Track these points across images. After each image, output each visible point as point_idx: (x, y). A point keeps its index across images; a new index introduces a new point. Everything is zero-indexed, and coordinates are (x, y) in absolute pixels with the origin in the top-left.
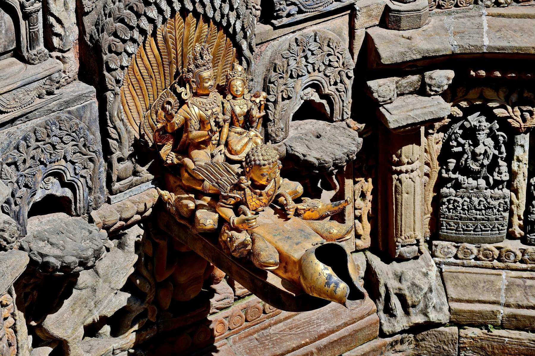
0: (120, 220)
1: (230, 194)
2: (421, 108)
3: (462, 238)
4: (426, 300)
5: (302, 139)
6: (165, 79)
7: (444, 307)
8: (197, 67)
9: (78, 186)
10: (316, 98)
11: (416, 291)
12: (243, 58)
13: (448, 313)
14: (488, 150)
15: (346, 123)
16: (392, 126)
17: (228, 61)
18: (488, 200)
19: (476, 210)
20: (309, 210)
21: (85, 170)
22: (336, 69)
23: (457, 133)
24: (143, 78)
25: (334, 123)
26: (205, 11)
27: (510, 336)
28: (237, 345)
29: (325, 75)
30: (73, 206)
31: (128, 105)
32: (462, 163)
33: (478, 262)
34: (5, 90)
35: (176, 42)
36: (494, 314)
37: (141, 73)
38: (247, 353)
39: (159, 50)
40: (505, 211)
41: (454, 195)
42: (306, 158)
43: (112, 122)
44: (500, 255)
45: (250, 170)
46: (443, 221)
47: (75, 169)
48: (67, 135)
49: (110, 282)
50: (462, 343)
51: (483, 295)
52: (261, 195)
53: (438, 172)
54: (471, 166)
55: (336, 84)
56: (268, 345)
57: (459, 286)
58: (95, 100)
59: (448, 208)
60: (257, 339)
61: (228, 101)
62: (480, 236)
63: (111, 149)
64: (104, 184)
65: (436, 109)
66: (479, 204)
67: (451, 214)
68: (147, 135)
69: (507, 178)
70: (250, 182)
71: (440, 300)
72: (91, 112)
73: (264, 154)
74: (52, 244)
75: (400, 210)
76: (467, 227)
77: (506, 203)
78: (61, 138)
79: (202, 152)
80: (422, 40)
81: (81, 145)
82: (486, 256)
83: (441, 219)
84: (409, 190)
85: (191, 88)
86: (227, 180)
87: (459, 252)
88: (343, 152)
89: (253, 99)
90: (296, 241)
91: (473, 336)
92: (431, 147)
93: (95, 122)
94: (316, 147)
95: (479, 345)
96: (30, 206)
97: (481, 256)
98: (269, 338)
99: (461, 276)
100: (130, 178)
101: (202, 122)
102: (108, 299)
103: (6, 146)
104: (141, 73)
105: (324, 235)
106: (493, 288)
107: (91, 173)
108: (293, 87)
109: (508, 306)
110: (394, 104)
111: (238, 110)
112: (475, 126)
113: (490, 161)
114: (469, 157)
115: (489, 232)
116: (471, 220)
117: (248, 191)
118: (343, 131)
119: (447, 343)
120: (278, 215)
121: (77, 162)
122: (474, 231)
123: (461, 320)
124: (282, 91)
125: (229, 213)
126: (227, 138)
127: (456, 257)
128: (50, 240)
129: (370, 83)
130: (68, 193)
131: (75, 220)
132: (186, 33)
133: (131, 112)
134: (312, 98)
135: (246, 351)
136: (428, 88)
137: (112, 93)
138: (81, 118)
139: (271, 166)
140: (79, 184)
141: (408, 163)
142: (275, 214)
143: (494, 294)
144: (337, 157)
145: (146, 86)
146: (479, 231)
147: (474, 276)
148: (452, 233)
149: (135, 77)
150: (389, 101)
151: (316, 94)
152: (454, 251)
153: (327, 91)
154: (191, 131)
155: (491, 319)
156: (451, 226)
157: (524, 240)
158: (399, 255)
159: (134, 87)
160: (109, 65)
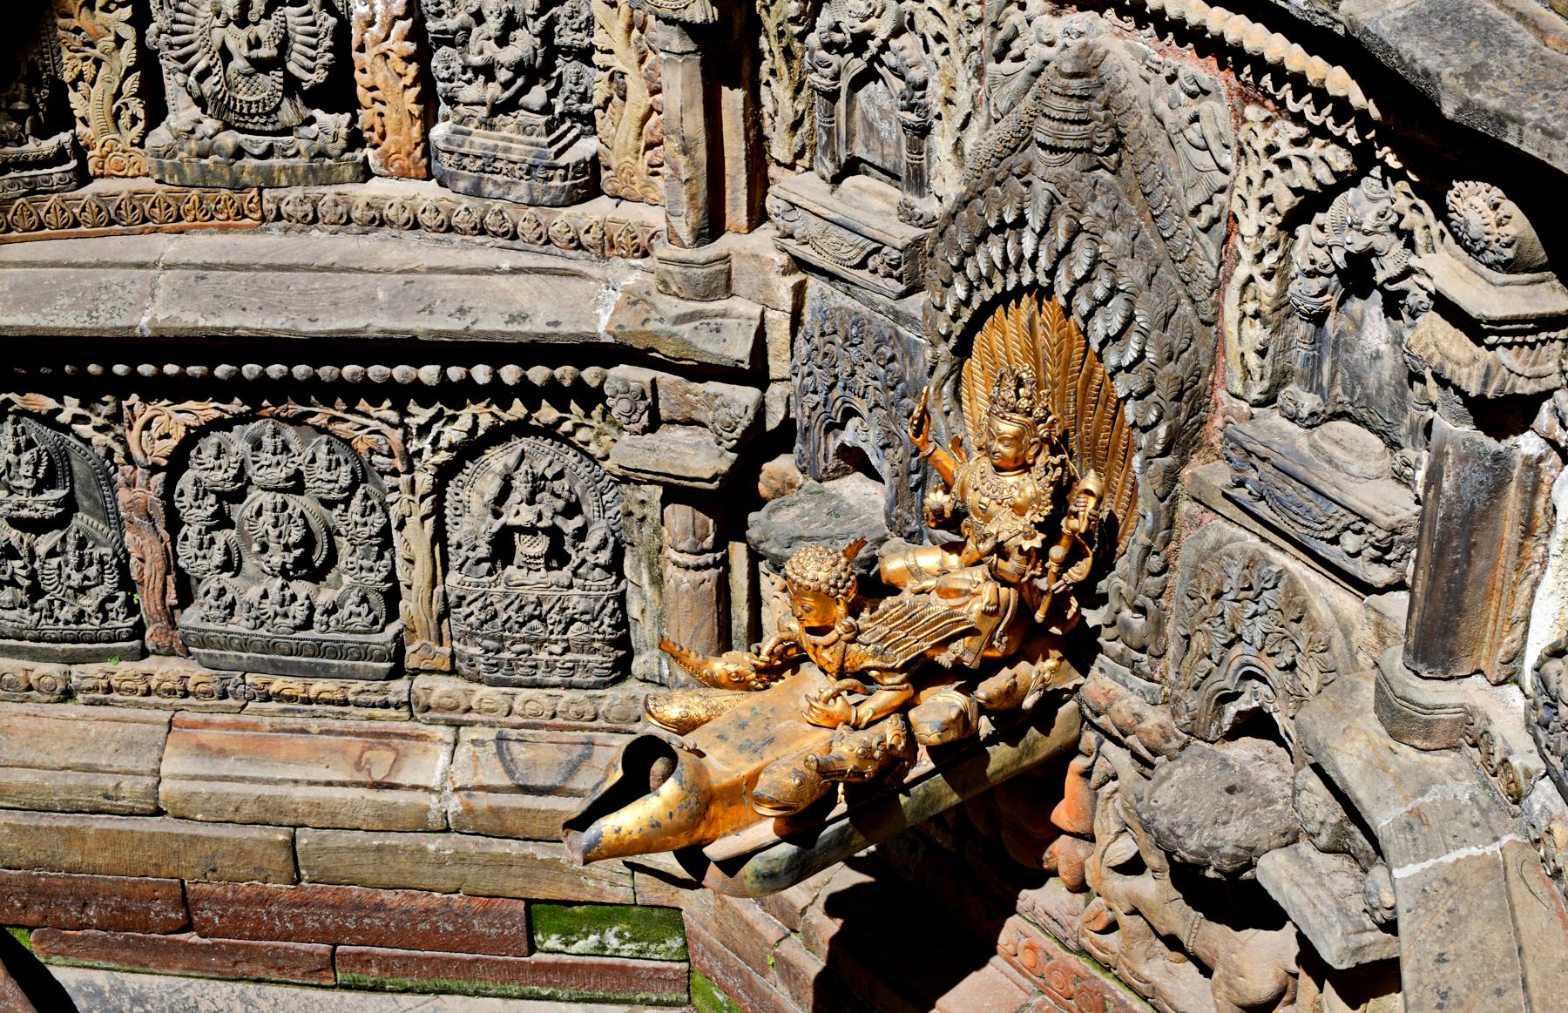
34: (815, 210)
80: (1359, 757)
96: (838, 443)
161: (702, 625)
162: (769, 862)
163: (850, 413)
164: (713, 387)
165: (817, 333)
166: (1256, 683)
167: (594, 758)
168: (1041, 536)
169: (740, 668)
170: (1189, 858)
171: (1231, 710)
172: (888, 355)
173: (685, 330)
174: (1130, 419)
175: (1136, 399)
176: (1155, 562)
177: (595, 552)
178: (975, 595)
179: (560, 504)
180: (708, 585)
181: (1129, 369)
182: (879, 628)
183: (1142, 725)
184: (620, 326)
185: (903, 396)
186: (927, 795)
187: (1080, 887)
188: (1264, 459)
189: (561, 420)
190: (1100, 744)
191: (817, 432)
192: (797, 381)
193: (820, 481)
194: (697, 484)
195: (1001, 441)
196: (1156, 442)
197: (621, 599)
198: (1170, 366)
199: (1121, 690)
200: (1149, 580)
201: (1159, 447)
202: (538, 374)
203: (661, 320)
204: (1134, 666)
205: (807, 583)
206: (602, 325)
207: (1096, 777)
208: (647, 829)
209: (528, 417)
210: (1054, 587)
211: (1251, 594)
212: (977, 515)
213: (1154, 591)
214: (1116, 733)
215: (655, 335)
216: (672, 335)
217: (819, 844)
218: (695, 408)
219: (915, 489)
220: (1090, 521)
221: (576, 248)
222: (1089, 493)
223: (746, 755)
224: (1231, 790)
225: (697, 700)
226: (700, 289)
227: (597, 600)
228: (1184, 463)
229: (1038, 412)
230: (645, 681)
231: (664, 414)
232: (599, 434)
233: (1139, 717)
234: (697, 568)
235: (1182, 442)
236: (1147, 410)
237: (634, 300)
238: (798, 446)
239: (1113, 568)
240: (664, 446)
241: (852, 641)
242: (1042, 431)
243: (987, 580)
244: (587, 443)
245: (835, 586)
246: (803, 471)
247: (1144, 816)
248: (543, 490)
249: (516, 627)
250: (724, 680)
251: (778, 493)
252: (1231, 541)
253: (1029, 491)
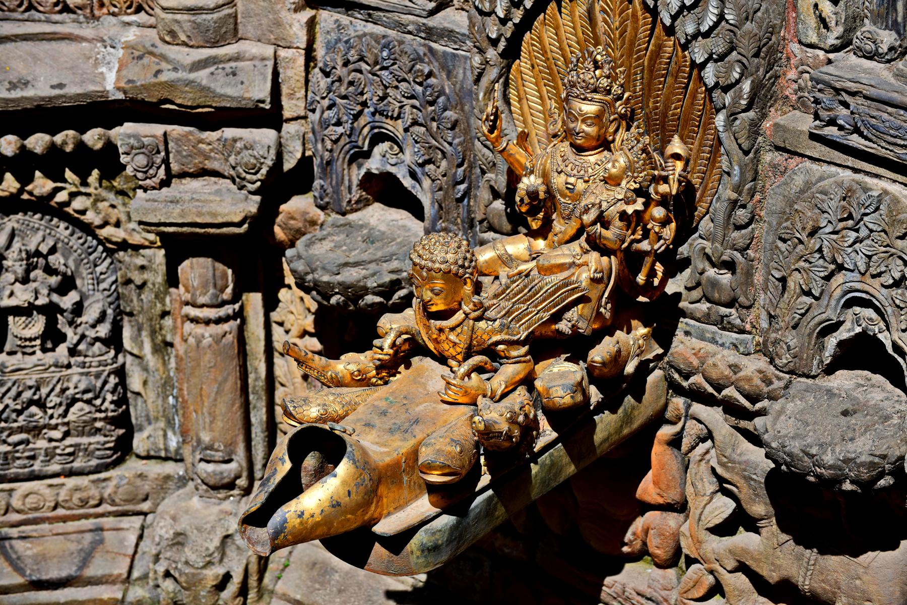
26: (656, 6)
48: (404, 80)
96: (363, 172)
103: (333, 41)
107: (440, 177)
134: (880, 336)
161: (225, 380)
162: (433, 534)
163: (378, 138)
164: (229, 133)
165: (340, 62)
166: (857, 309)
167: (107, 540)
168: (641, 200)
169: (361, 367)
170: (826, 473)
171: (831, 342)
172: (426, 71)
173: (202, 76)
174: (710, 80)
175: (716, 61)
176: (741, 215)
177: (94, 326)
178: (579, 266)
179: (54, 280)
180: (230, 337)
181: (706, 35)
182: (503, 304)
183: (741, 374)
184: (129, 81)
185: (445, 110)
186: (553, 464)
187: (675, 559)
188: (853, 94)
189: (57, 190)
190: (689, 407)
191: (340, 165)
192: (315, 117)
193: (344, 214)
194: (225, 230)
195: (583, 121)
196: (741, 97)
197: (121, 373)
198: (748, 25)
199: (711, 347)
200: (736, 234)
201: (744, 102)
202: (38, 142)
203: (175, 69)
204: (723, 323)
205: (437, 265)
206: (110, 82)
207: (686, 443)
208: (328, 510)
209: (21, 191)
210: (656, 247)
211: (850, 223)
212: (564, 196)
213: (741, 243)
214: (710, 390)
215: (170, 85)
216: (189, 83)
217: (472, 515)
218: (207, 157)
219: (460, 200)
220: (680, 182)
221: (60, 12)
222: (677, 157)
223: (398, 436)
224: (845, 413)
225: (331, 398)
226: (210, 34)
227: (98, 376)
228: (764, 116)
229: (616, 89)
230: (148, 457)
231: (175, 167)
232: (96, 201)
233: (735, 368)
234: (219, 321)
235: (762, 98)
236: (730, 69)
237: (137, 53)
238: (317, 183)
239: (696, 230)
240: (187, 197)
241: (479, 319)
242: (621, 109)
243: (586, 252)
244: (83, 212)
245: (463, 266)
246: (322, 208)
247: (774, 445)
248: (35, 267)
249: (14, 416)
250: (348, 378)
251: (300, 233)
252: (821, 179)
253: (622, 161)
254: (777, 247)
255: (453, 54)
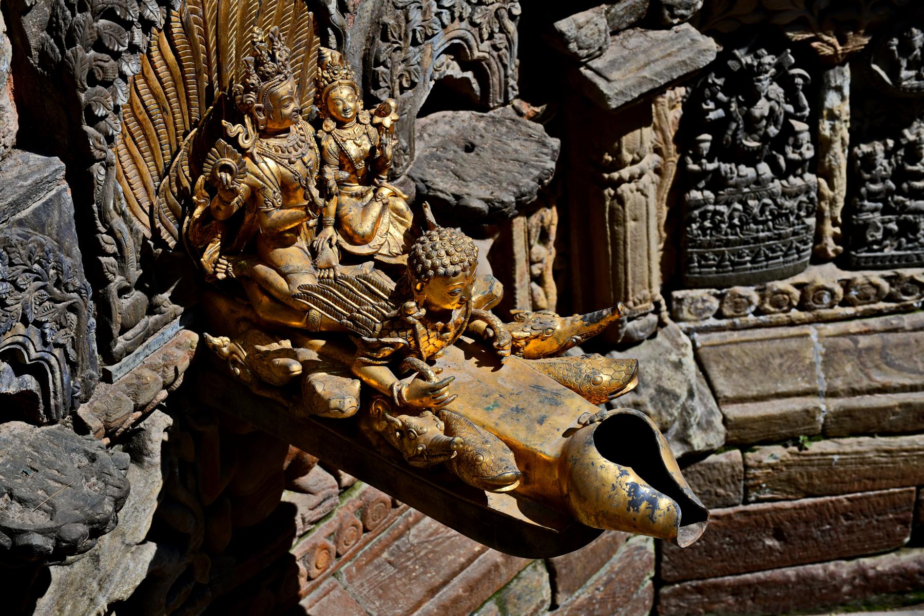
0: (136, 409)
1: (383, 340)
2: (663, 58)
3: (730, 278)
4: (685, 414)
5: (439, 159)
6: (189, 106)
7: (713, 419)
8: (264, 77)
9: (51, 367)
10: (455, 70)
11: (667, 403)
12: (329, 29)
13: (722, 428)
14: (777, 108)
15: (513, 107)
16: (613, 104)
17: (300, 40)
18: (779, 200)
19: (757, 222)
20: (536, 337)
21: (62, 332)
22: (490, 7)
23: (714, 84)
24: (150, 116)
25: (491, 113)
27: (841, 450)
28: (357, 583)
29: (473, 24)
30: (41, 406)
31: (127, 178)
32: (727, 140)
33: (762, 318)
35: (206, 29)
36: (809, 414)
37: (145, 106)
38: (380, 597)
39: (175, 51)
40: (808, 216)
41: (712, 201)
42: (463, 203)
43: (105, 222)
44: (803, 298)
45: (422, 287)
46: (692, 253)
47: (43, 336)
48: (25, 271)
49: (123, 535)
50: (752, 479)
51: (783, 382)
52: (445, 330)
53: (676, 161)
54: (744, 142)
55: (491, 37)
56: (414, 570)
57: (732, 372)
58: (65, 185)
59: (702, 228)
60: (390, 562)
61: (329, 133)
62: (765, 269)
63: (106, 276)
64: (95, 346)
65: (691, 55)
66: (762, 211)
67: (708, 238)
68: (166, 228)
69: (809, 154)
70: (423, 312)
71: (705, 405)
72: (60, 212)
73: (452, 250)
74: (21, 501)
75: (622, 253)
76: (740, 256)
77: (811, 200)
78: (14, 283)
79: (292, 249)
81: (50, 284)
82: (777, 304)
83: (689, 250)
84: (638, 212)
85: (255, 122)
86: (371, 311)
87: (725, 305)
88: (532, 176)
89: (377, 120)
90: (535, 415)
91: (772, 461)
92: (663, 116)
93: (69, 229)
94: (474, 173)
95: (783, 476)
97: (767, 306)
98: (412, 554)
99: (734, 350)
100: (142, 323)
101: (286, 187)
102: (122, 566)
104: (145, 106)
105: (584, 389)
106: (800, 365)
107: (73, 334)
108: (418, 63)
109: (832, 394)
110: (608, 56)
111: (353, 150)
112: (751, 66)
113: (779, 127)
114: (741, 126)
115: (781, 259)
116: (746, 242)
117: (420, 327)
118: (514, 127)
119: (722, 483)
120: (474, 360)
121: (47, 321)
122: (752, 262)
123: (747, 437)
124: (401, 76)
125: (383, 375)
126: (338, 209)
127: (719, 315)
128: (16, 492)
129: (563, 25)
130: (31, 383)
131: (50, 433)
132: (222, 7)
133: (132, 189)
135: (376, 593)
136: (667, 13)
137: (102, 165)
138: (41, 227)
139: (468, 272)
140: (53, 361)
141: (634, 162)
142: (468, 357)
143: (803, 378)
144: (524, 189)
145: (156, 130)
146: (761, 262)
147: (759, 346)
148: (710, 273)
149: (135, 116)
150: (598, 53)
151: (455, 63)
152: (715, 304)
153: (477, 54)
154: (267, 212)
155: (804, 424)
156: (710, 260)
157: (843, 262)
158: (624, 337)
159: (133, 139)
160: (93, 112)
254: (383, 72)
255: (43, 204)
